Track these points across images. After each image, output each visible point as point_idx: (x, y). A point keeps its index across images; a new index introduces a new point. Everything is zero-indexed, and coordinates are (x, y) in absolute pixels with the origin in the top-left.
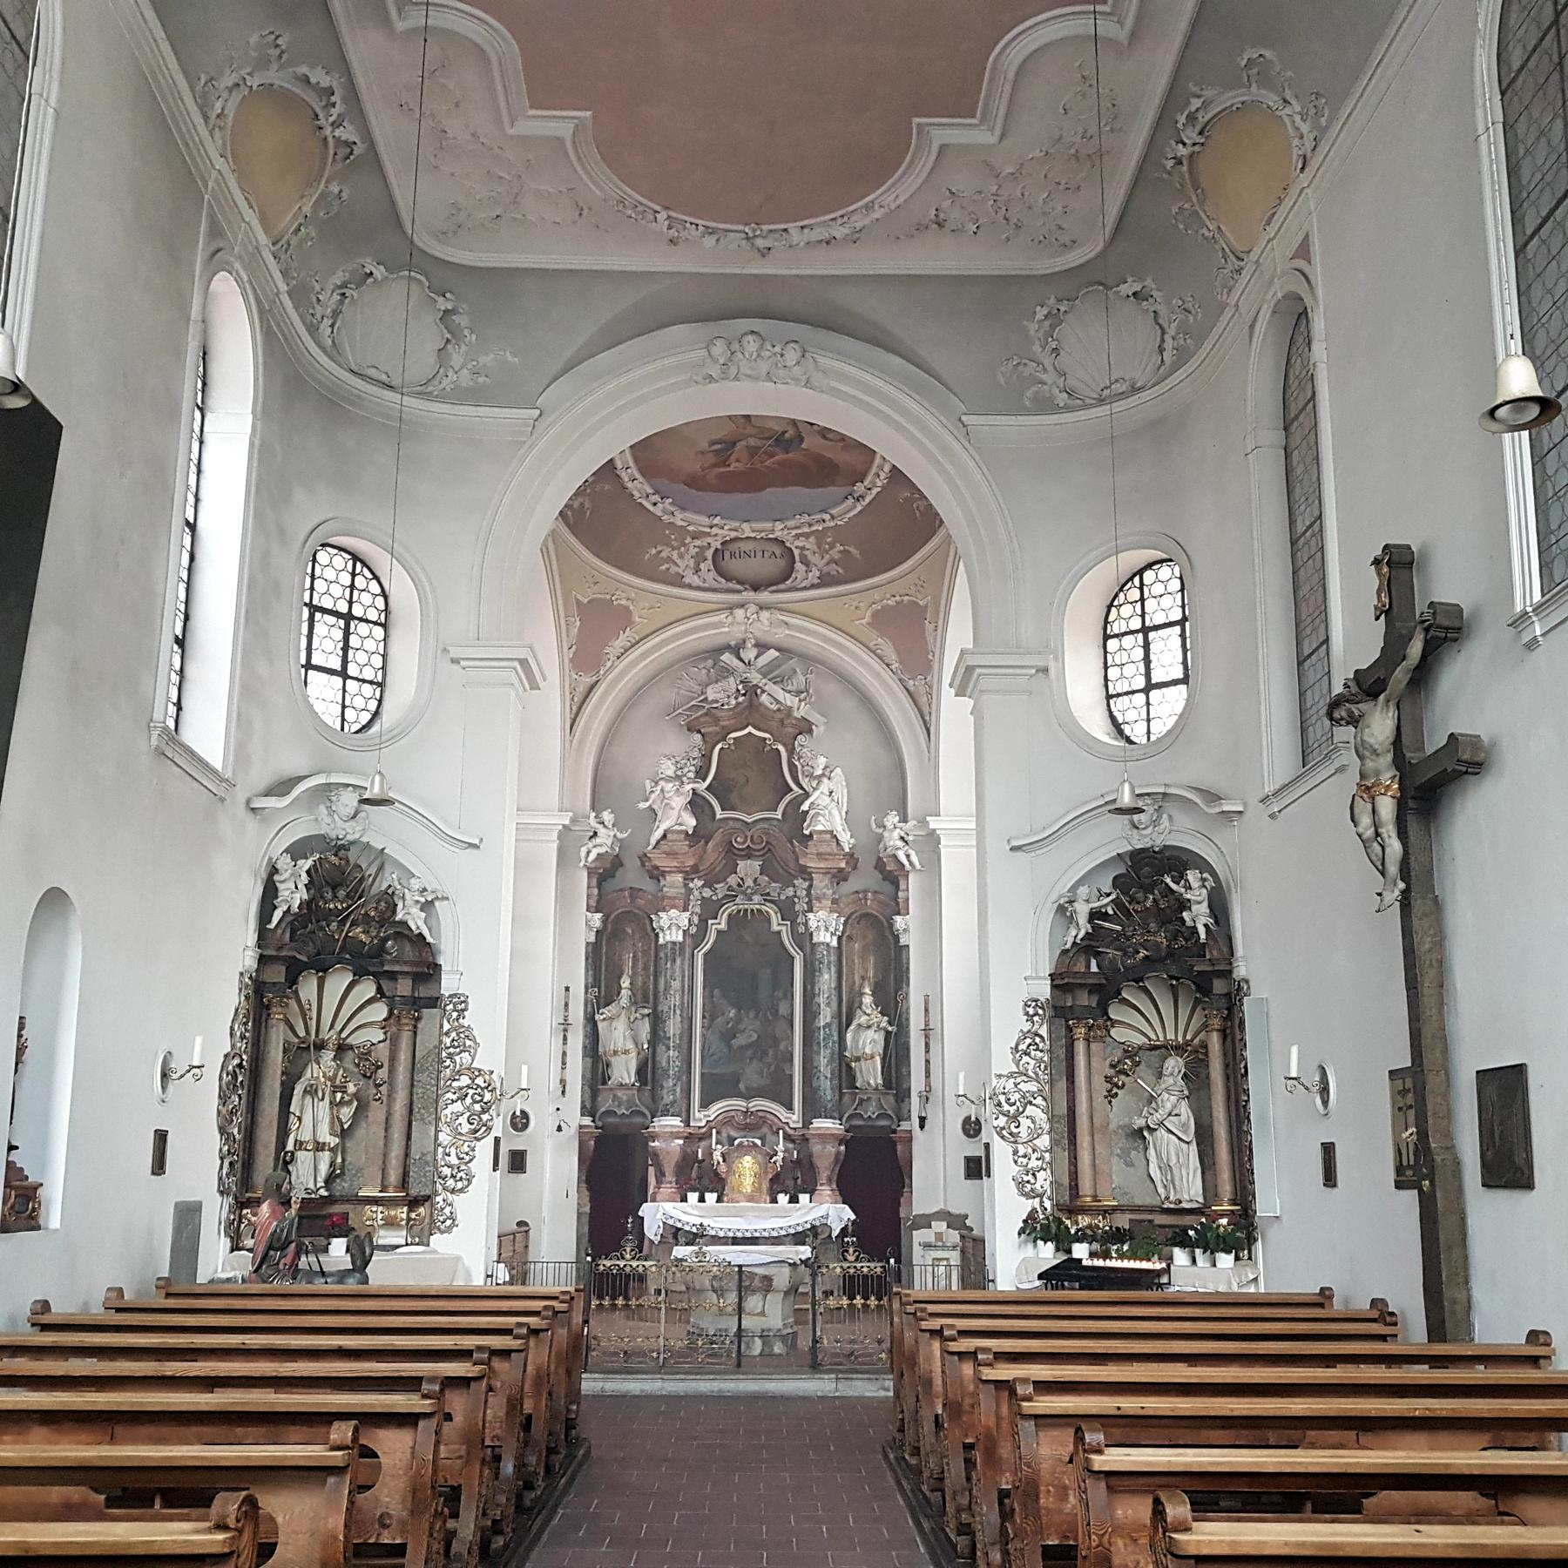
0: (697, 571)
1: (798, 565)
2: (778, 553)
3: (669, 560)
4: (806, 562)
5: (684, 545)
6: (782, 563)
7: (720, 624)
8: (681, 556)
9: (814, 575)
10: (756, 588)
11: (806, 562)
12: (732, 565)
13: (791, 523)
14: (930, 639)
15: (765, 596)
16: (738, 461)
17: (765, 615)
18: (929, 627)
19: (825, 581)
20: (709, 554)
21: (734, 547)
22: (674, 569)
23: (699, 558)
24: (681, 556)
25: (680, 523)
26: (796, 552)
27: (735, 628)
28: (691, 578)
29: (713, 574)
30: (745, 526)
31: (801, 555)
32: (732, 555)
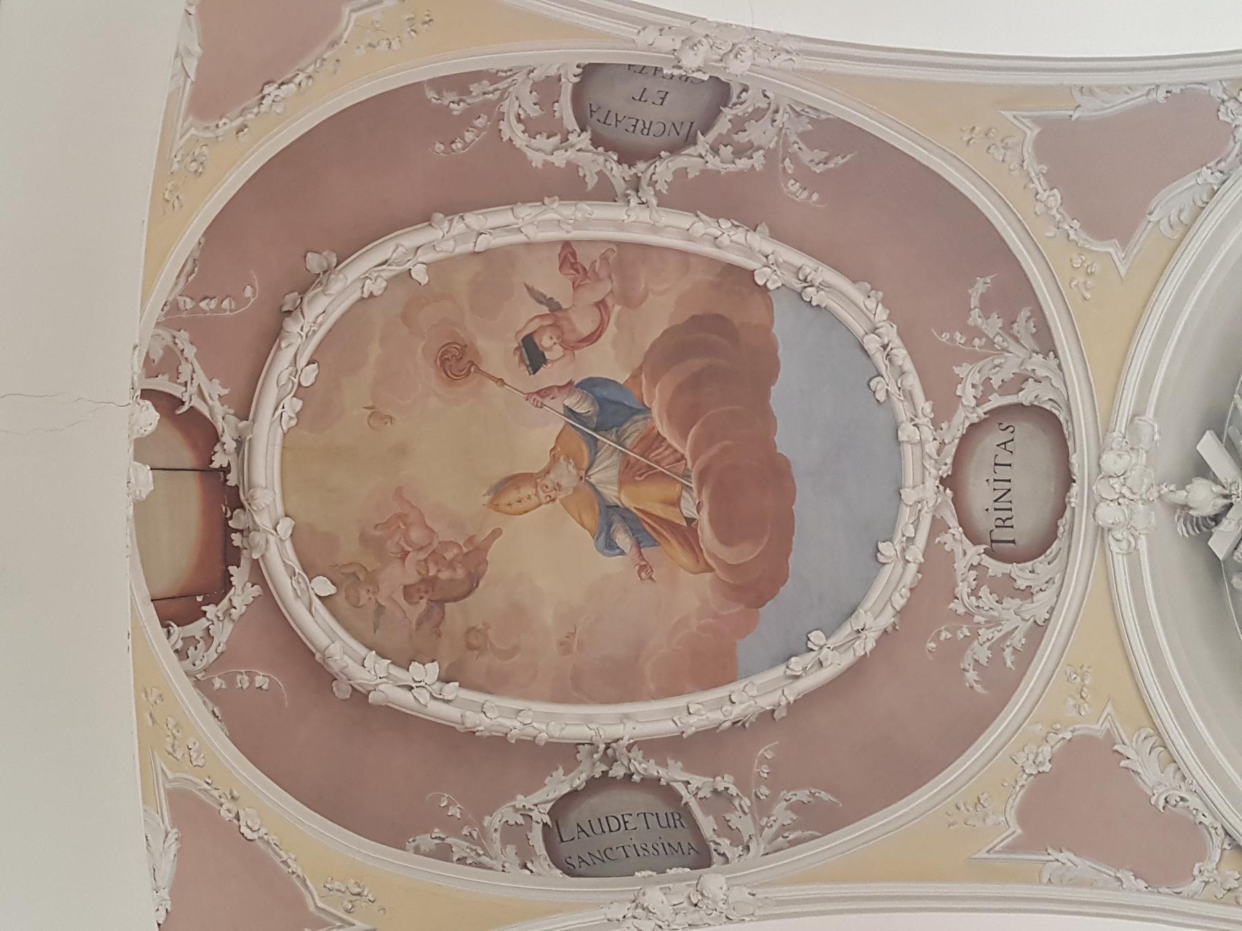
0: (1027, 593)
1: (1025, 397)
2: (1003, 437)
3: (997, 648)
4: (1021, 379)
5: (969, 614)
6: (1024, 429)
7: (1132, 554)
8: (993, 623)
9: (1037, 363)
10: (1068, 480)
11: (1021, 379)
12: (1026, 523)
13: (902, 410)
14: (1121, 103)
15: (1080, 462)
16: (676, 503)
17: (1110, 462)
18: (1090, 109)
19: (1046, 344)
20: (996, 568)
21: (985, 522)
22: (1019, 639)
23: (1006, 589)
24: (993, 623)
25: (887, 619)
26: (996, 401)
27: (1140, 523)
28: (1037, 608)
29: (1040, 564)
30: (909, 495)
31: (1005, 388)
32: (1003, 524)
